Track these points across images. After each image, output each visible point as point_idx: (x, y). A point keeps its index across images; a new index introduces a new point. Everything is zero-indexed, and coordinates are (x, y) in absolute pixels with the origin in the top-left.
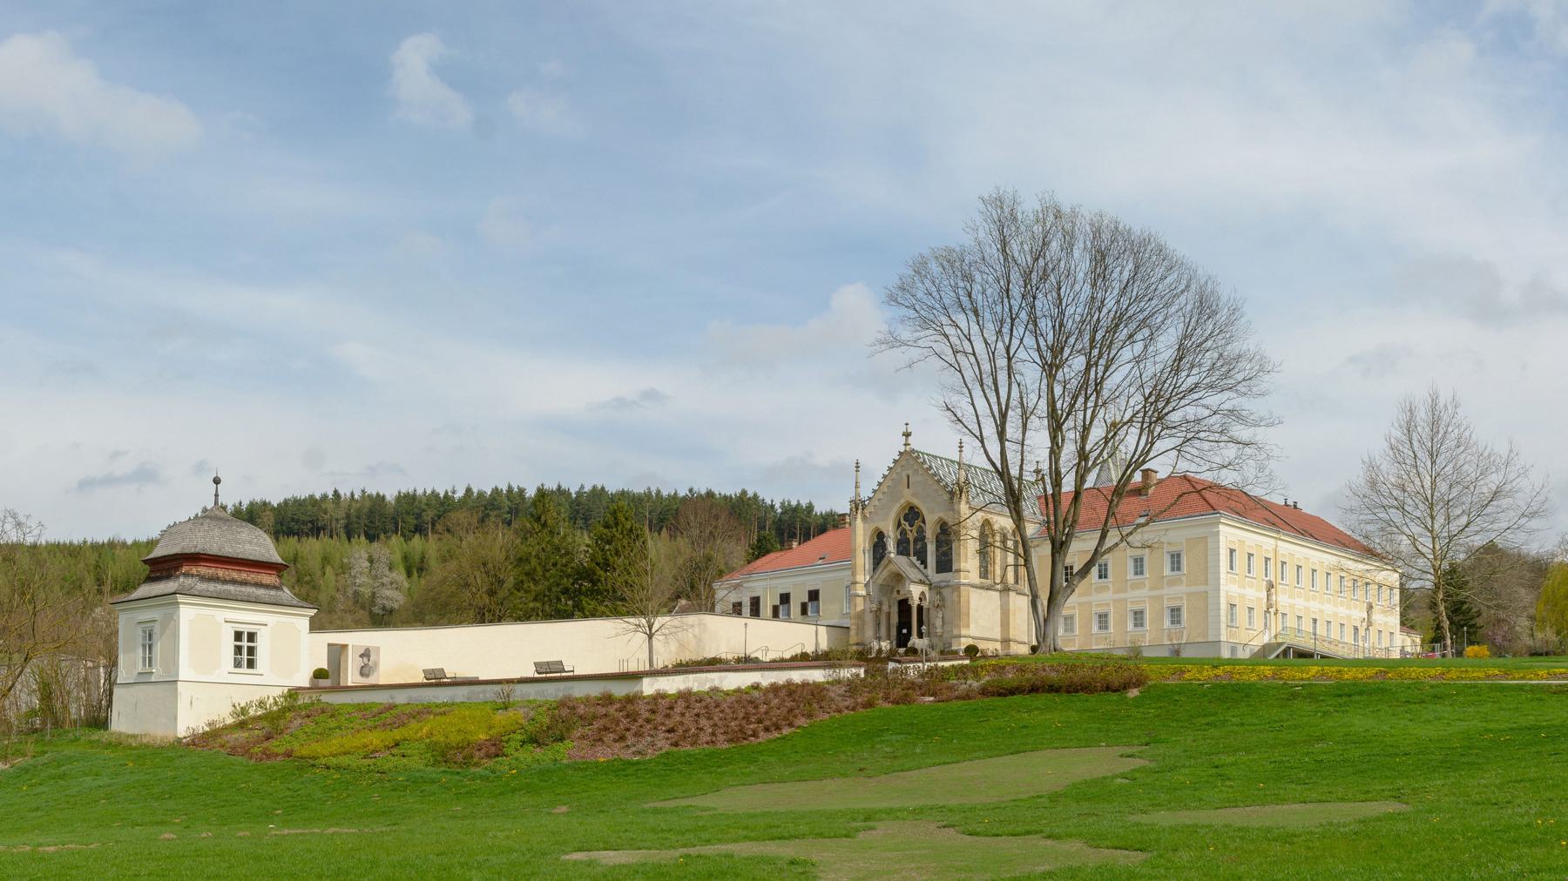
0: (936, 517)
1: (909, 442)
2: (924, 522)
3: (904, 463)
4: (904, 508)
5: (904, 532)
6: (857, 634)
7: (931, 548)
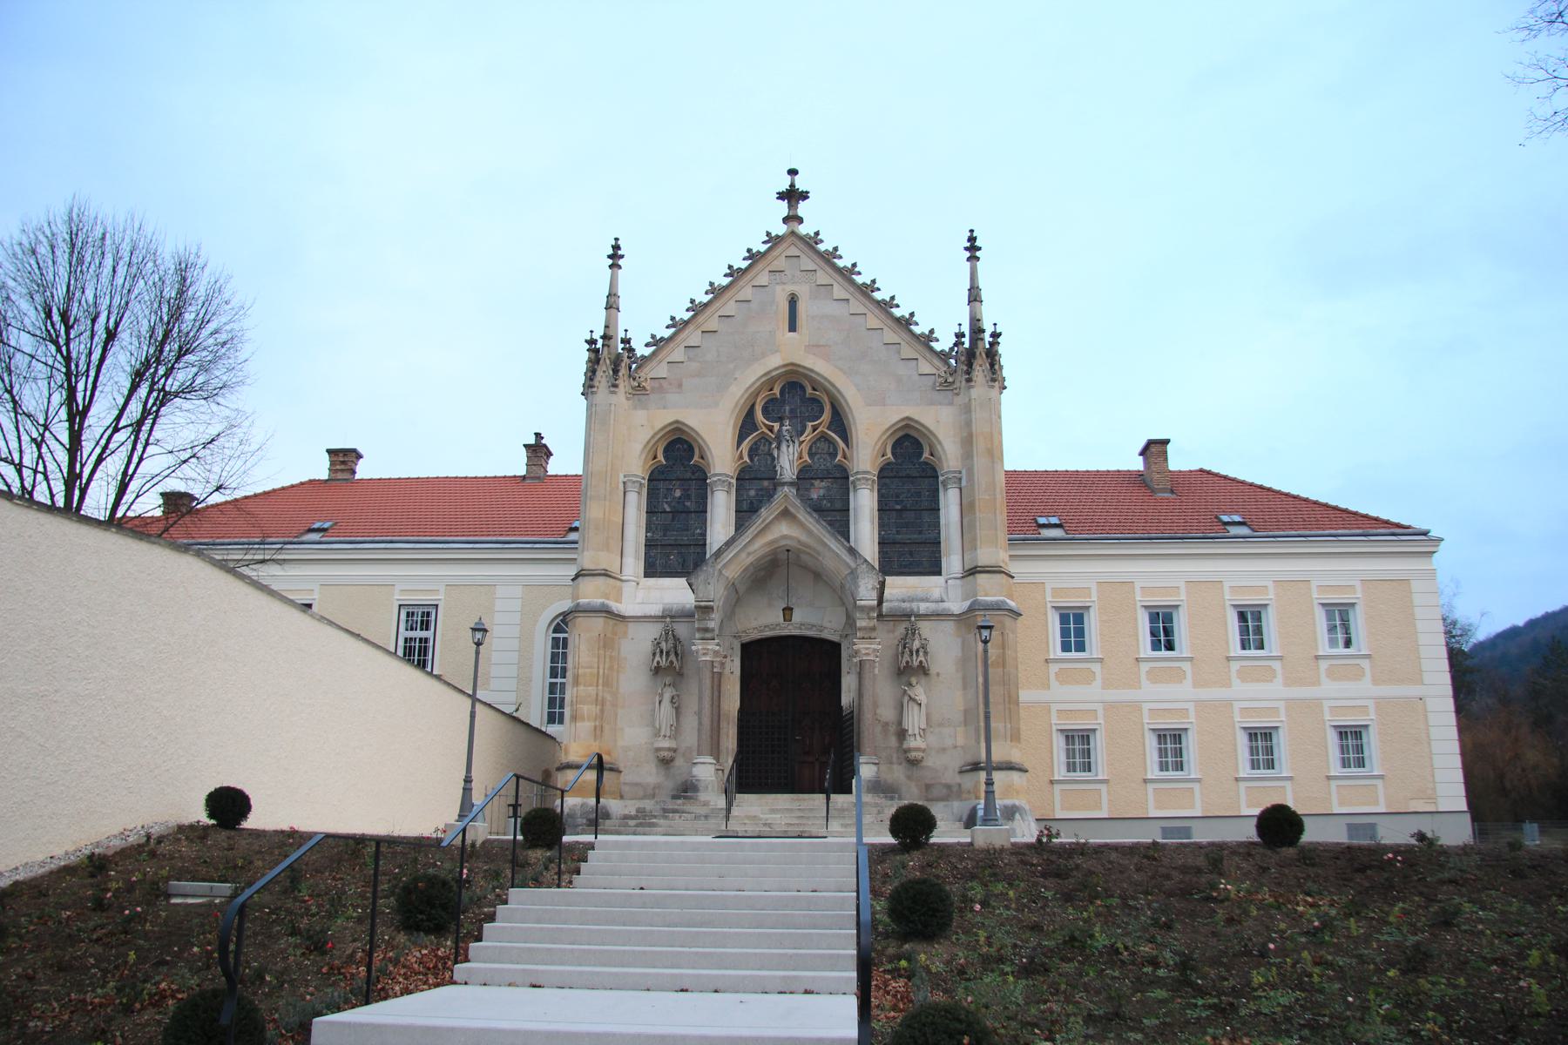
0: (893, 415)
1: (800, 212)
2: (840, 424)
4: (769, 383)
5: (763, 448)
6: (598, 732)
7: (865, 503)
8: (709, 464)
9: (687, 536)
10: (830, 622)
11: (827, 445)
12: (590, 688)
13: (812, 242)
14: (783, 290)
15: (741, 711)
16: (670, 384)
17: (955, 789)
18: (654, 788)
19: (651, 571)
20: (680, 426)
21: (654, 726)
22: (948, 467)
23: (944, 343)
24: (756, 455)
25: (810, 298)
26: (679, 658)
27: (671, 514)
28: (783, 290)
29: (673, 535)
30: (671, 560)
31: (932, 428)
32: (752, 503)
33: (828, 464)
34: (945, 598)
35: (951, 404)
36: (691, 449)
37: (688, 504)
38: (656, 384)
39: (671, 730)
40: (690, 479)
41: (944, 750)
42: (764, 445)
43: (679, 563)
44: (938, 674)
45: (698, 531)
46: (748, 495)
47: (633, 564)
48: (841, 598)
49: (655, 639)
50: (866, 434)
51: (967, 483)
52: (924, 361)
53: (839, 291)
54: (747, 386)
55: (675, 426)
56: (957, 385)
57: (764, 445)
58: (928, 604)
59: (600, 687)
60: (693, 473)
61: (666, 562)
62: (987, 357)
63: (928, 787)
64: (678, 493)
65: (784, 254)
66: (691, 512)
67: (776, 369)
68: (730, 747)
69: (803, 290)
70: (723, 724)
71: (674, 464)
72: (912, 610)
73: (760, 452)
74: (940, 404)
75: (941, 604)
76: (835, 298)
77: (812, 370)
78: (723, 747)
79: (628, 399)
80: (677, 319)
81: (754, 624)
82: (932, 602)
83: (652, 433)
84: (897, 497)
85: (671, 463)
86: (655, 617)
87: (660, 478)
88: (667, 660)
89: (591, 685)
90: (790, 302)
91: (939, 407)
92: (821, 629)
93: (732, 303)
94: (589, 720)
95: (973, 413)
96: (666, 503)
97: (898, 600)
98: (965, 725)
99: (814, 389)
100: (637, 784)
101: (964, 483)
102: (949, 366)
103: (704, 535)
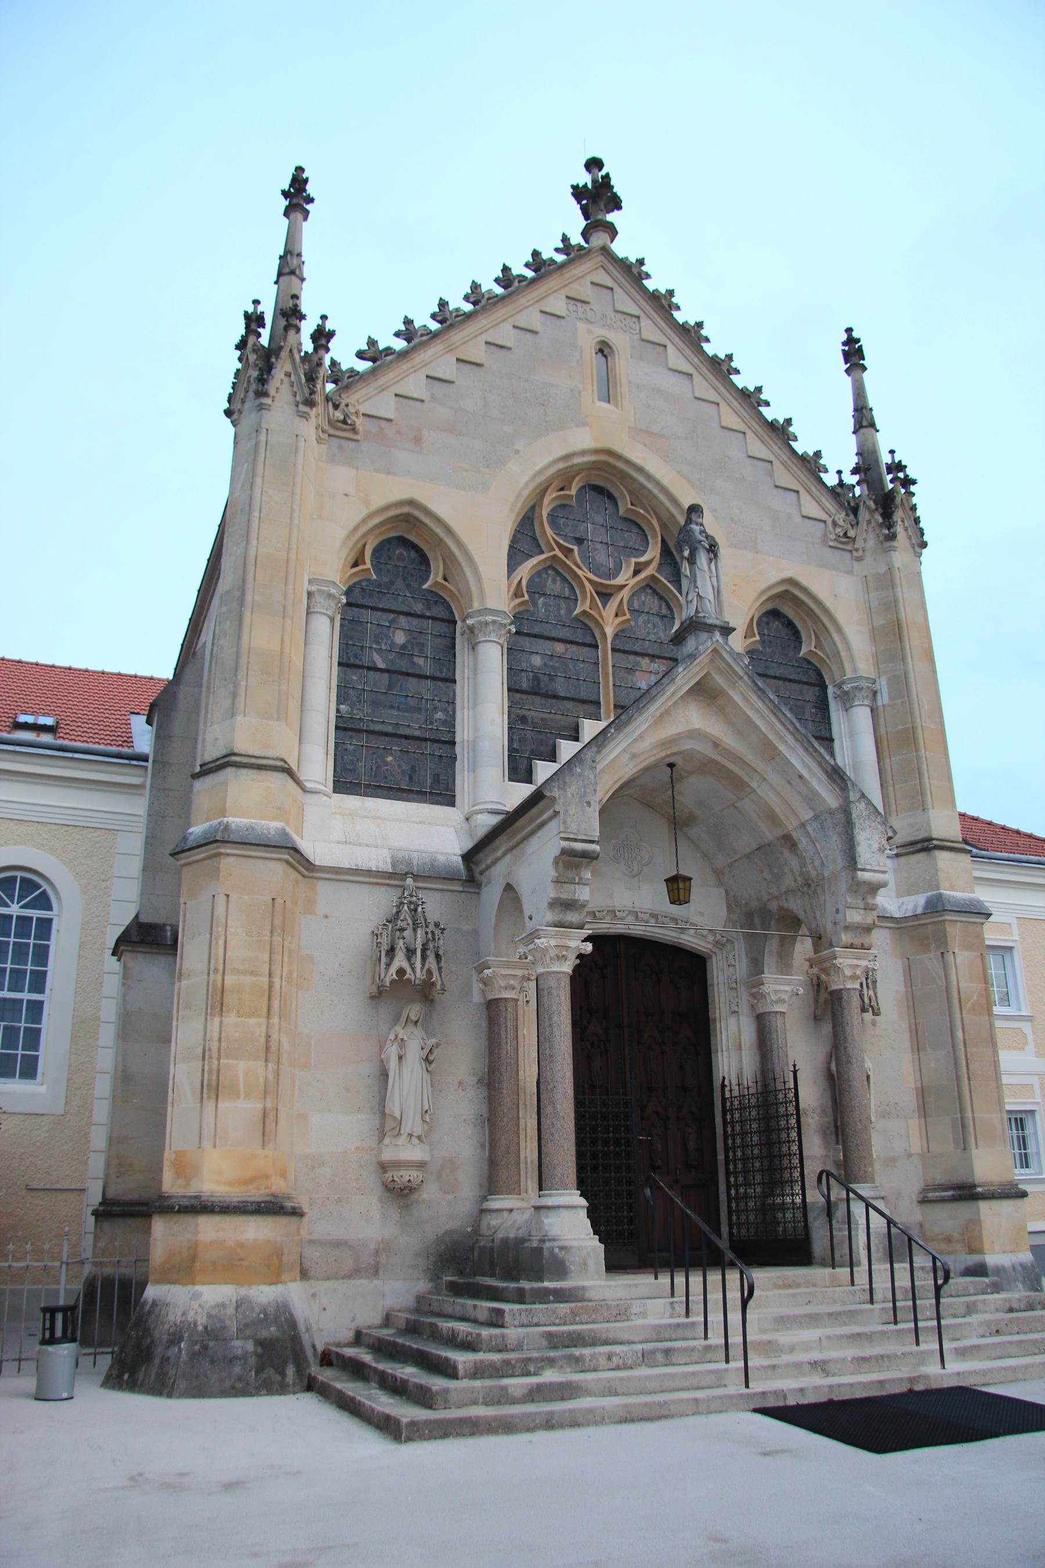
10: (701, 914)
12: (252, 1021)
16: (399, 432)
22: (855, 670)
27: (386, 676)
30: (386, 763)
32: (536, 679)
35: (850, 572)
37: (421, 661)
38: (372, 426)
43: (403, 772)
45: (439, 715)
50: (733, 592)
51: (891, 699)
52: (808, 497)
54: (538, 468)
55: (406, 510)
59: (275, 1020)
61: (378, 767)
64: (400, 638)
67: (583, 453)
69: (619, 340)
76: (670, 366)
77: (640, 469)
79: (319, 441)
83: (364, 513)
85: (386, 579)
86: (379, 874)
87: (365, 602)
89: (252, 1015)
91: (834, 573)
93: (507, 327)
94: (247, 1096)
95: (899, 589)
101: (883, 699)
103: (450, 723)
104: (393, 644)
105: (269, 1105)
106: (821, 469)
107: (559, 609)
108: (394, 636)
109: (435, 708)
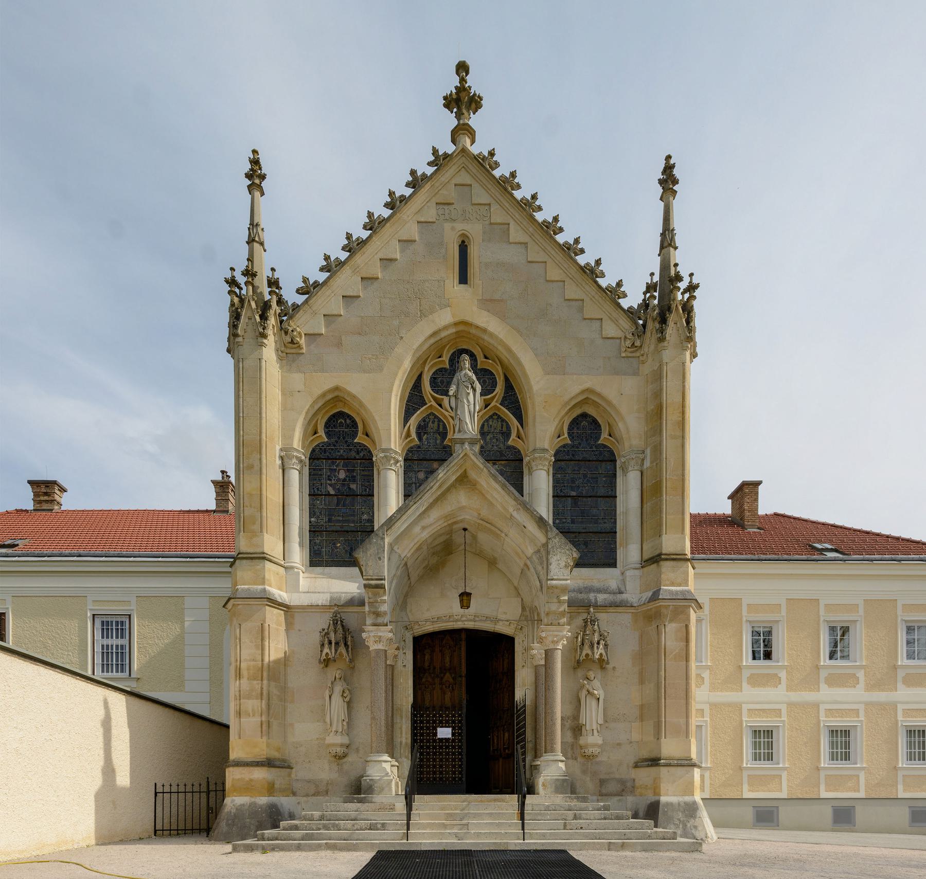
3: (449, 193)
6: (266, 728)
8: (373, 442)
9: (353, 522)
10: (505, 613)
11: (499, 423)
13: (486, 163)
14: (453, 229)
15: (414, 706)
17: (629, 784)
18: (327, 784)
19: (317, 559)
20: (341, 394)
21: (325, 722)
23: (633, 298)
24: (425, 433)
25: (483, 241)
26: (350, 649)
28: (453, 229)
29: (339, 521)
30: (337, 548)
31: (614, 402)
33: (501, 445)
34: (623, 589)
35: (636, 373)
36: (354, 424)
37: (353, 486)
39: (343, 725)
40: (355, 459)
41: (619, 744)
42: (433, 422)
43: (346, 551)
44: (614, 668)
46: (417, 478)
47: (298, 555)
48: (516, 588)
49: (323, 630)
51: (652, 462)
53: (516, 233)
56: (645, 349)
57: (433, 422)
58: (606, 596)
60: (358, 453)
61: (333, 550)
62: (683, 311)
63: (602, 782)
64: (342, 475)
65: (453, 182)
66: (358, 495)
68: (404, 741)
70: (397, 720)
71: (337, 442)
72: (590, 601)
73: (429, 430)
74: (625, 374)
75: (618, 595)
78: (397, 740)
80: (332, 259)
81: (427, 615)
82: (609, 593)
84: (573, 481)
85: (333, 440)
88: (336, 653)
90: (460, 246)
92: (496, 620)
96: (331, 485)
97: (574, 591)
98: (642, 722)
99: (486, 357)
100: (309, 781)
101: (647, 464)
102: (636, 324)
104: (339, 480)
105: (264, 719)
106: (621, 296)
107: (436, 439)
108: (339, 474)
109: (363, 513)
